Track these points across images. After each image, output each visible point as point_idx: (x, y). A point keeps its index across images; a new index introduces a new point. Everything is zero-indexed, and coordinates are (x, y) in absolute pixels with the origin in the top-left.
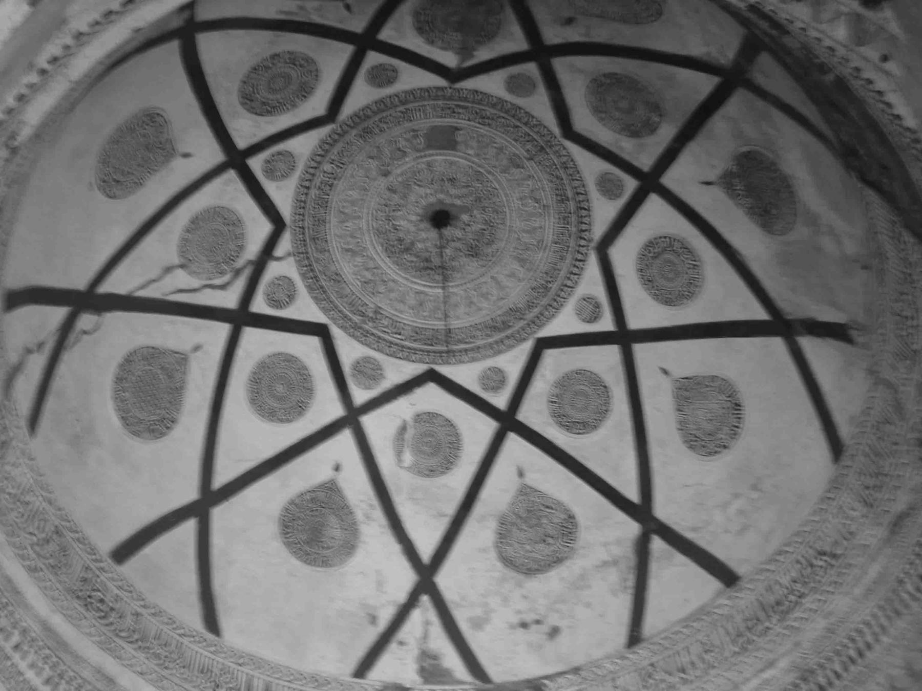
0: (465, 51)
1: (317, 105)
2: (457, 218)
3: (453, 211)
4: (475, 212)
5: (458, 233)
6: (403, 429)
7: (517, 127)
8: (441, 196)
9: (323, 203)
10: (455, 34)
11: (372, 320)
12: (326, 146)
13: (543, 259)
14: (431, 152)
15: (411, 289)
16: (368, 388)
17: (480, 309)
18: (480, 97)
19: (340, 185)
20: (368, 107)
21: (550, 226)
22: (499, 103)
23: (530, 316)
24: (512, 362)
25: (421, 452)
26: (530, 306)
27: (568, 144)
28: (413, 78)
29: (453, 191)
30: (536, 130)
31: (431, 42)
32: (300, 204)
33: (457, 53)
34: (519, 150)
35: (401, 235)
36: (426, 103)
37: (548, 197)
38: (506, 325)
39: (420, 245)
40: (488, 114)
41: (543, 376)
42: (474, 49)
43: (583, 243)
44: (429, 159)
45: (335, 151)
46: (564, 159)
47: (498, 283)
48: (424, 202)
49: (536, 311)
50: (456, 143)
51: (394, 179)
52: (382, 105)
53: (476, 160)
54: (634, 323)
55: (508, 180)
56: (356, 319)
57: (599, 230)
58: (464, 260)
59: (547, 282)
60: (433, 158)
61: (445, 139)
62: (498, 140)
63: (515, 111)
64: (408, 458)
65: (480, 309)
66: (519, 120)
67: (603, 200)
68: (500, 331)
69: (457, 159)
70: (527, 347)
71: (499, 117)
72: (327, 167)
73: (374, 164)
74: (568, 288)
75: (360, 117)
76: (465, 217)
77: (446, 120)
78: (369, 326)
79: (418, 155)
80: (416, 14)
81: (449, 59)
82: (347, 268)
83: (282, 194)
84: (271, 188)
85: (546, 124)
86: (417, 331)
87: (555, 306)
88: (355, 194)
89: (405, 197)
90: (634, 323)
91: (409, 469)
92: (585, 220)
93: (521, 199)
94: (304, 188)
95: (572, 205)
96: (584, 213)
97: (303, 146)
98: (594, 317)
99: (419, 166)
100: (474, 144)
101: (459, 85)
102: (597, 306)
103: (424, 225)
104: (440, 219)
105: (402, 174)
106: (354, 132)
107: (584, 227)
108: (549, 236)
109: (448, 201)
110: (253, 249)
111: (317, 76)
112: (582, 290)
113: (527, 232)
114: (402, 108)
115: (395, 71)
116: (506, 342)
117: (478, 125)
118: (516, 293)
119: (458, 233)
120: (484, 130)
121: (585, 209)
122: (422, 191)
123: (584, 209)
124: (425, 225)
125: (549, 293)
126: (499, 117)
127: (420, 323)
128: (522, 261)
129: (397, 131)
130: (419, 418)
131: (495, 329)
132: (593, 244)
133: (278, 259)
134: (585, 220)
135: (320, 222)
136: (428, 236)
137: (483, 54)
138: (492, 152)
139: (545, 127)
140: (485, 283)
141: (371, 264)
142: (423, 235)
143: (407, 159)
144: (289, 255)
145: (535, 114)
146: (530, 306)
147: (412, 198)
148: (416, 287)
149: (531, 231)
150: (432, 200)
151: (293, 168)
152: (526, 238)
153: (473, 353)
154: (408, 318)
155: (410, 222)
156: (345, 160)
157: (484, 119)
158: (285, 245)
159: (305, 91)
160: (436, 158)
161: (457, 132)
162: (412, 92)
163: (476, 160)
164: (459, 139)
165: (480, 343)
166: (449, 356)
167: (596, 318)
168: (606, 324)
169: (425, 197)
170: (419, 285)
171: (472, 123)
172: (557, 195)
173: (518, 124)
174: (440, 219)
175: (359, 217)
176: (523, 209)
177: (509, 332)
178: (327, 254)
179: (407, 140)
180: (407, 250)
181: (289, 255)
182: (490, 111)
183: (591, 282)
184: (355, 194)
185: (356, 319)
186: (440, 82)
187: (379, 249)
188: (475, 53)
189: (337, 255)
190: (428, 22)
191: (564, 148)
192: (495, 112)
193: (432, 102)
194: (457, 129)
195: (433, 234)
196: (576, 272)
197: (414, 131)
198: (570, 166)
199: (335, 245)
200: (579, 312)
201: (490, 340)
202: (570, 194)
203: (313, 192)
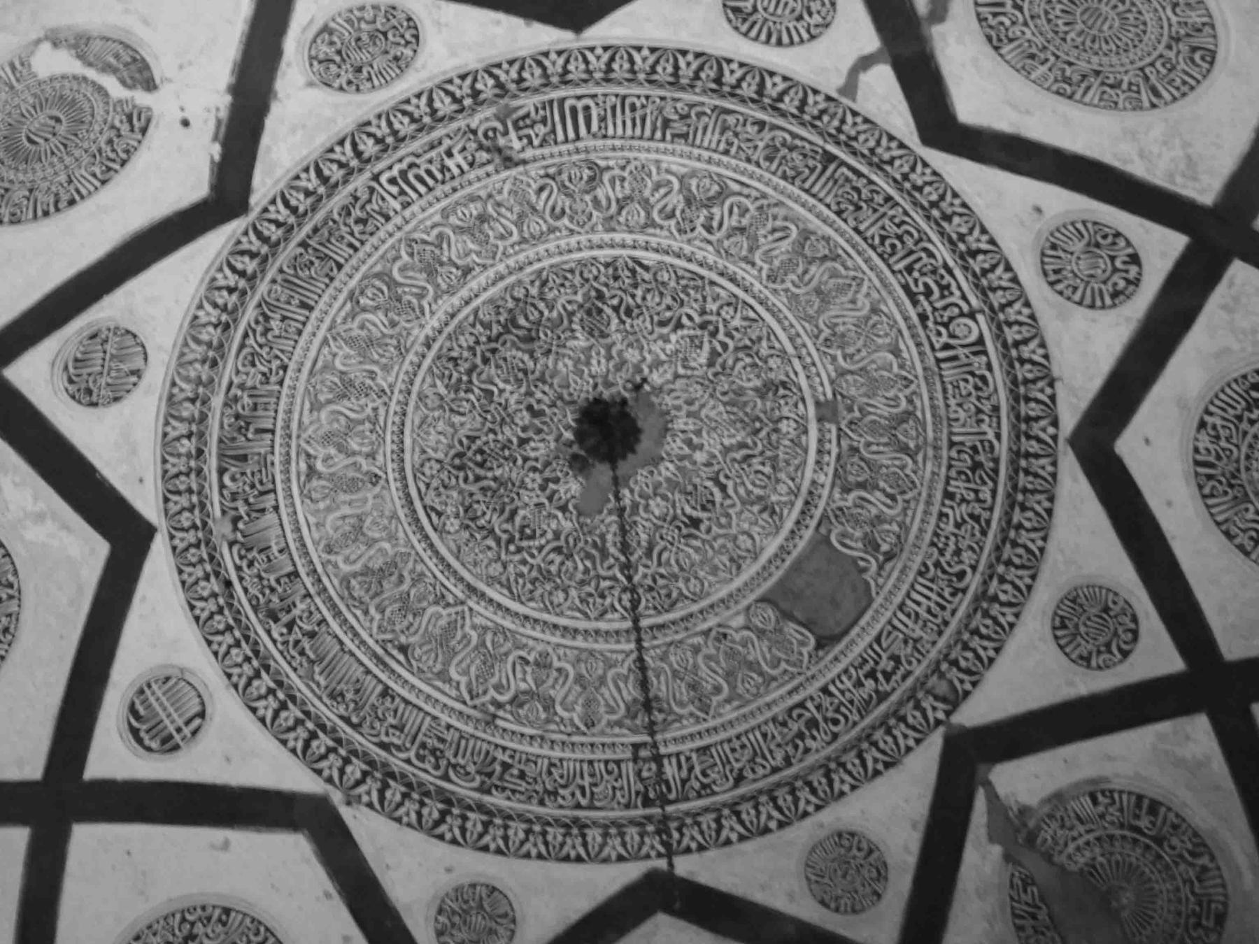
0: (1017, 830)
1: (1156, 447)
2: (579, 464)
3: (602, 472)
4: (567, 525)
5: (539, 449)
6: (140, 74)
7: (740, 779)
8: (667, 470)
9: (886, 247)
10: (1082, 860)
11: (490, 134)
12: (1033, 378)
13: (359, 633)
14: (801, 545)
15: (485, 267)
16: (326, 29)
17: (316, 406)
18: (873, 759)
19: (897, 308)
20: (1044, 529)
21: (434, 699)
22: (828, 785)
23: (221, 529)
24: (122, 442)
25: (40, 105)
26: (248, 546)
27: (632, 872)
28: (1027, 672)
29: (657, 507)
30: (707, 820)
31: (1096, 791)
32: (945, 208)
33: (1024, 811)
34: (679, 738)
35: (642, 323)
36: (942, 643)
37: (516, 737)
38: (232, 457)
39: (581, 341)
40: (810, 743)
41: (40, 517)
42: (1008, 857)
43: (355, 770)
44: (789, 525)
45: (998, 378)
46: (594, 835)
47: (352, 486)
48: (679, 424)
49: (228, 559)
50: (787, 616)
51: (801, 421)
52: (1020, 553)
53: (712, 622)
54: (89, 842)
55: (610, 665)
56: (528, 103)
57: (369, 829)
58: (469, 423)
59: (290, 626)
60: (785, 532)
61: (813, 600)
62: (729, 713)
63: (783, 802)
64: (53, 63)
65: (316, 406)
66: (753, 798)
67: (446, 882)
68: (226, 440)
69: (738, 582)
70: (146, 501)
71: (788, 761)
72: (969, 330)
73: (881, 410)
74: (253, 677)
75: (1030, 500)
76: (572, 487)
77: (862, 645)
78: (482, 118)
79: (818, 513)
80: (1200, 845)
81: (1022, 781)
82: (675, 160)
83: (1014, 208)
84: (1061, 202)
85: (711, 854)
86: (364, 217)
87: (217, 619)
88: (844, 315)
89: (736, 398)
90: (89, 842)
91: (19, 66)
92: (411, 807)
93: (543, 664)
94: (978, 252)
95: (463, 789)
96: (433, 809)
97: (1086, 346)
98: (145, 729)
99: (782, 488)
100: (759, 651)
101: (935, 742)
102: (169, 746)
103: (620, 379)
104: (609, 431)
105: (798, 444)
106: (1003, 450)
107: (395, 792)
108: (410, 684)
109: (642, 479)
110: (959, 51)
111: (1227, 534)
112: (227, 707)
113: (451, 627)
114: (973, 582)
115: (1086, 660)
116: (187, 446)
117: (797, 698)
118: (303, 522)
119: (539, 449)
120: (779, 698)
121: (437, 824)
122: (712, 443)
123: (442, 816)
124: (620, 387)
125: (255, 616)
126: (788, 761)
127: (386, 238)
128: (376, 576)
129: (920, 524)
130: (139, 122)
131: (242, 423)
132: (337, 797)
133: (865, 63)
134: (411, 807)
135: (852, 205)
136: (585, 367)
137: (981, 861)
138: (709, 677)
139: (701, 848)
140: (371, 456)
141: (636, 214)
142: (598, 366)
143: (826, 479)
144: (850, 88)
145: (748, 846)
146: (248, 546)
147: (714, 410)
148: (482, 280)
149: (444, 640)
150: (675, 446)
151: (1054, 278)
152: (436, 616)
153: (210, 336)
154: (424, 214)
155: (656, 358)
156: (949, 372)
157: (804, 722)
158: (884, 98)
159: (1215, 477)
160: (779, 540)
161: (812, 641)
162: (1000, 635)
163: (712, 622)
164: (791, 628)
165: (228, 371)
166: (240, 275)
167: (135, 732)
168: (112, 756)
169: (694, 434)
170: (484, 288)
171: (813, 689)
172: (506, 766)
173: (742, 790)
174: (609, 431)
175: (772, 278)
176: (517, 650)
177: (213, 462)
178: (758, 155)
179: (879, 519)
180: (593, 311)
181: (850, 88)
182: (819, 749)
183: (238, 749)
184: (844, 315)
185: (528, 103)
186: (974, 713)
187: (650, 258)
188: (997, 850)
189: (730, 169)
190: (1159, 841)
191: (621, 858)
192: (811, 759)
193: (933, 654)
194: (823, 643)
195: (583, 389)
196: (281, 714)
197: (889, 556)
198: (566, 841)
199: (766, 182)
200: (171, 680)
201: (217, 401)
202: (496, 800)
203: (943, 252)
